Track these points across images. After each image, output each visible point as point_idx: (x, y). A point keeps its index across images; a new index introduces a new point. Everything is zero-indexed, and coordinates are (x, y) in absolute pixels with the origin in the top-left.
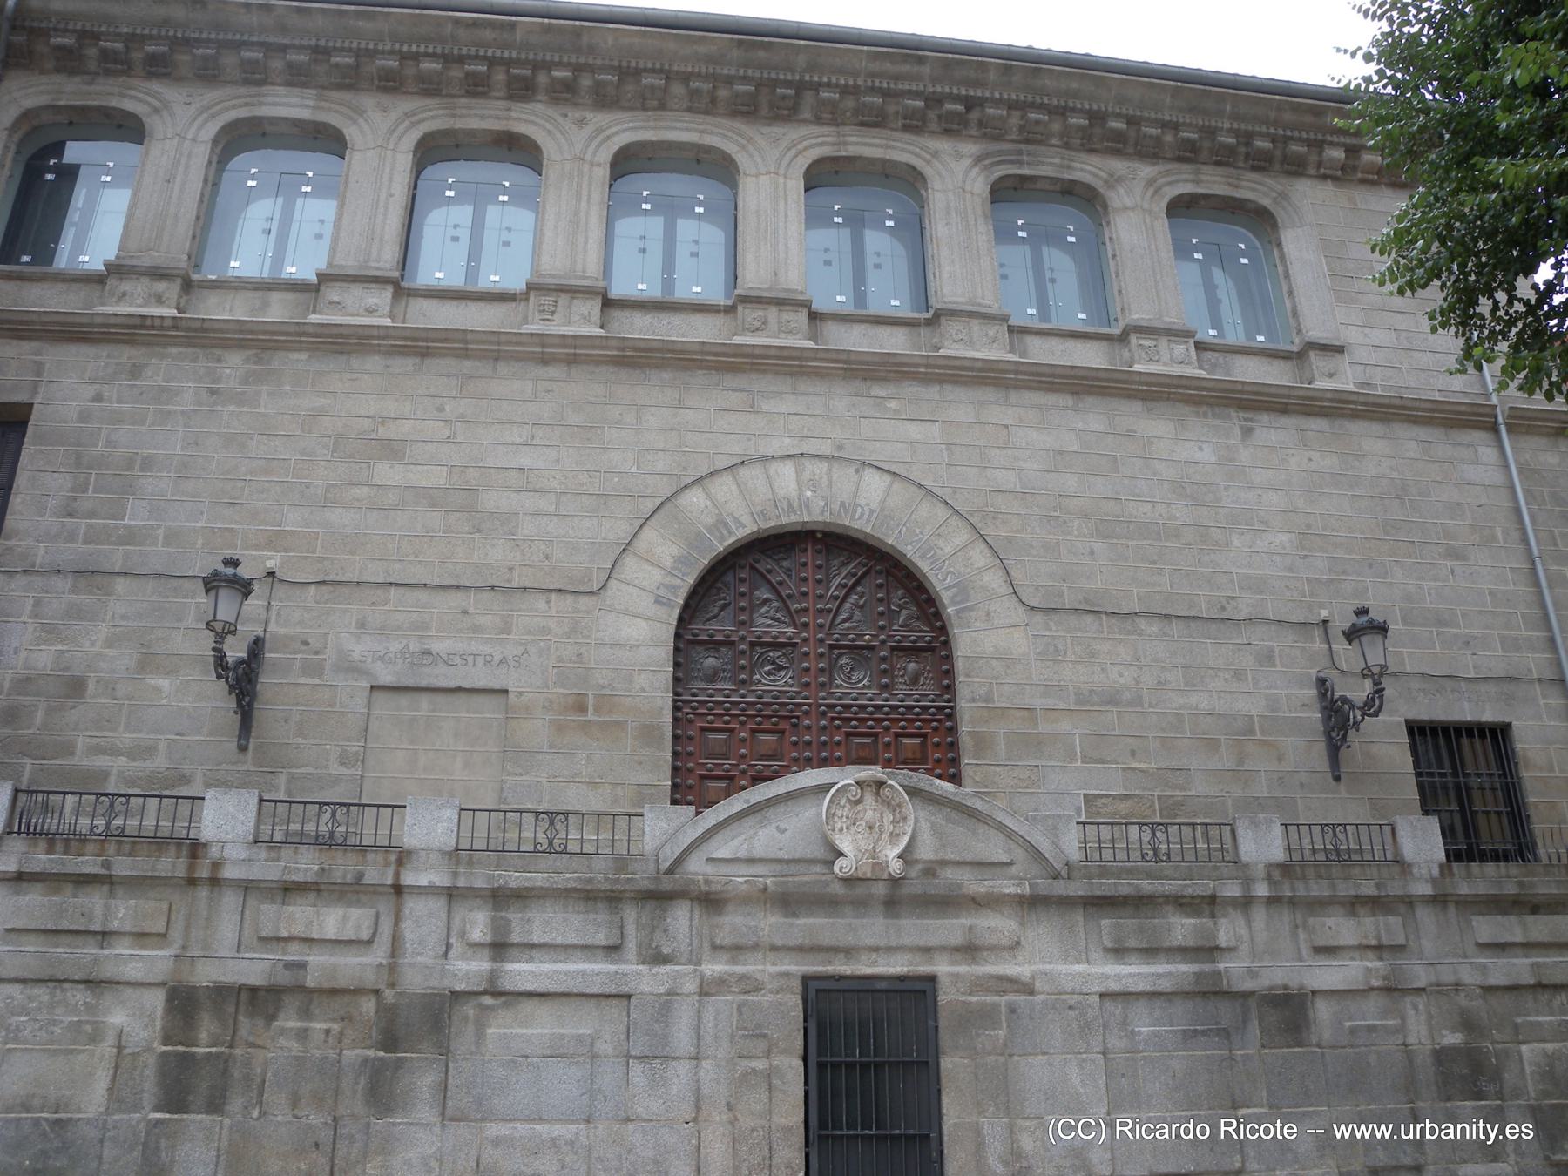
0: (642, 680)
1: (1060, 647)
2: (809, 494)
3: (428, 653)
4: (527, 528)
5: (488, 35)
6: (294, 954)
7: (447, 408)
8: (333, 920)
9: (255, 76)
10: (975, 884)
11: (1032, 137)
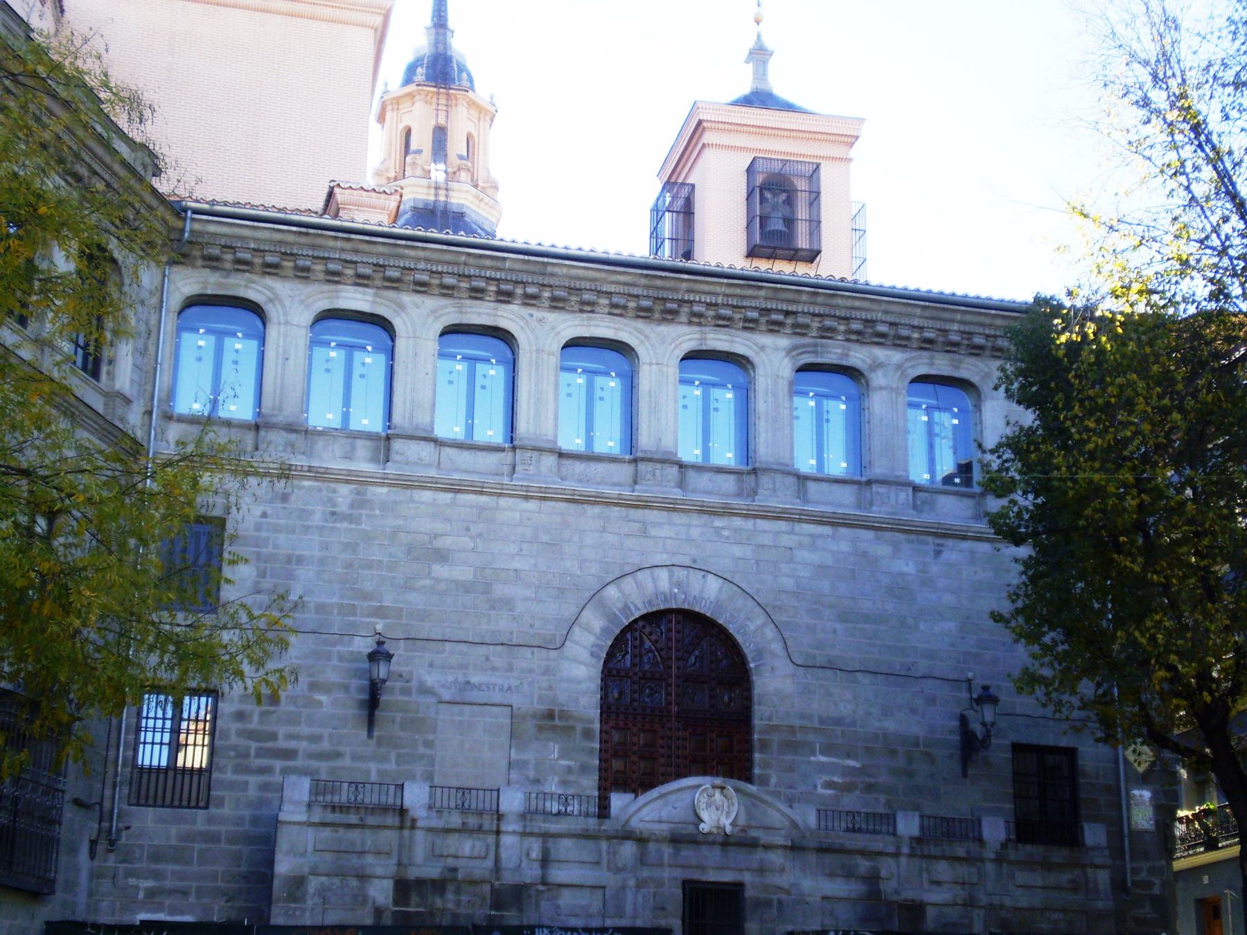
0: (584, 701)
2: (676, 590)
3: (468, 683)
4: (520, 608)
5: (488, 263)
6: (451, 862)
7: (472, 528)
8: (468, 846)
9: (333, 277)
10: (764, 837)
11: (827, 333)
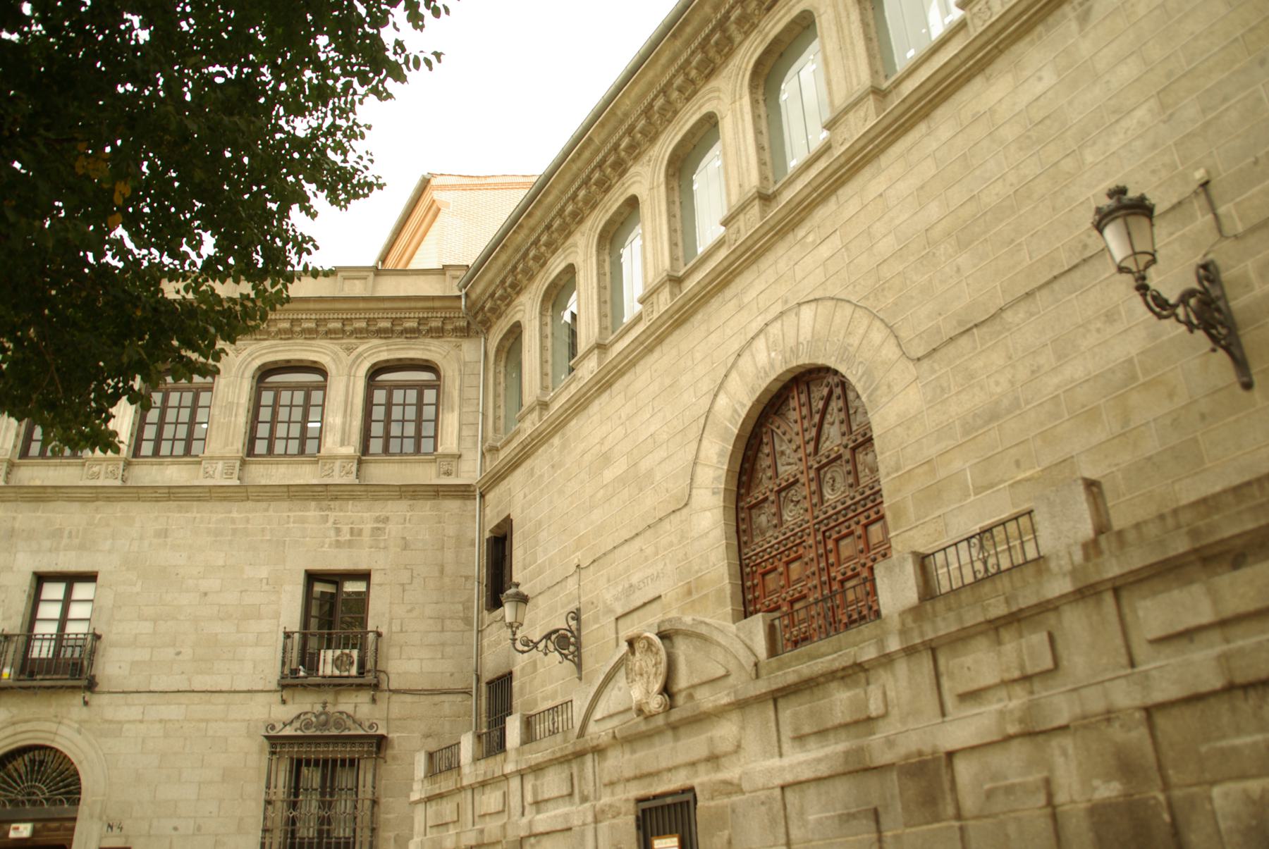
1: (945, 385)
5: (587, 154)
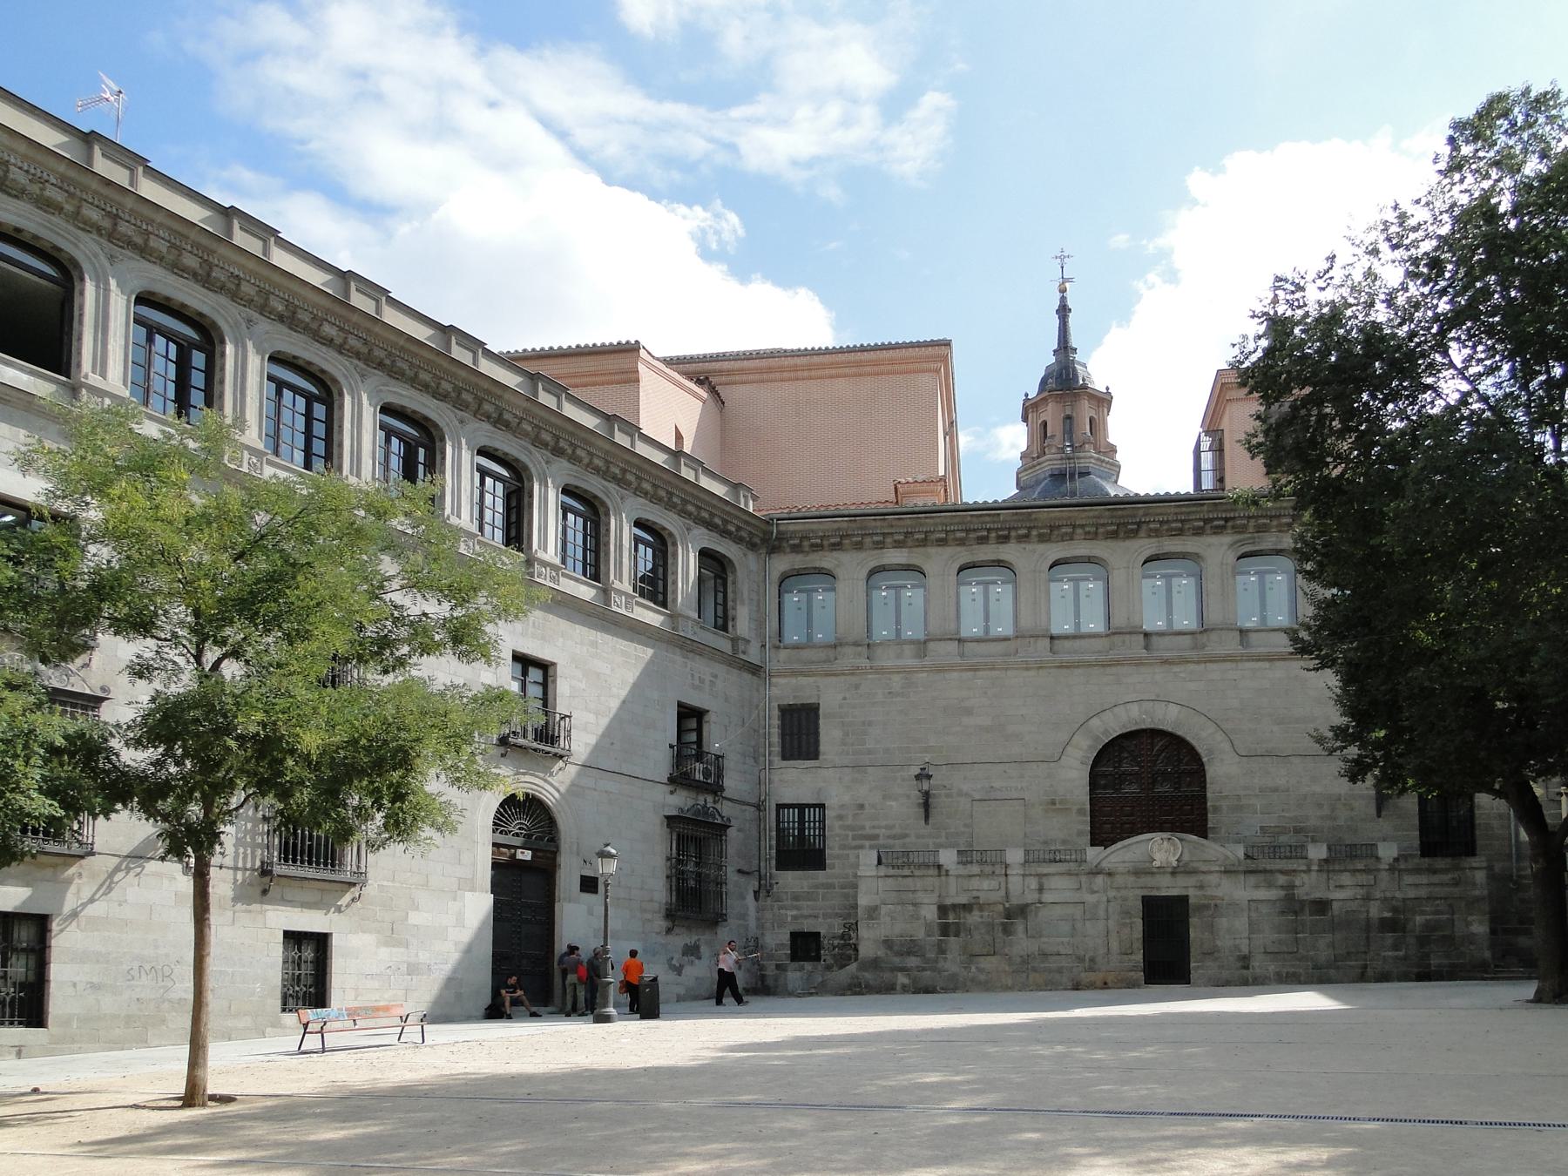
5: (987, 519)
9: (880, 545)
